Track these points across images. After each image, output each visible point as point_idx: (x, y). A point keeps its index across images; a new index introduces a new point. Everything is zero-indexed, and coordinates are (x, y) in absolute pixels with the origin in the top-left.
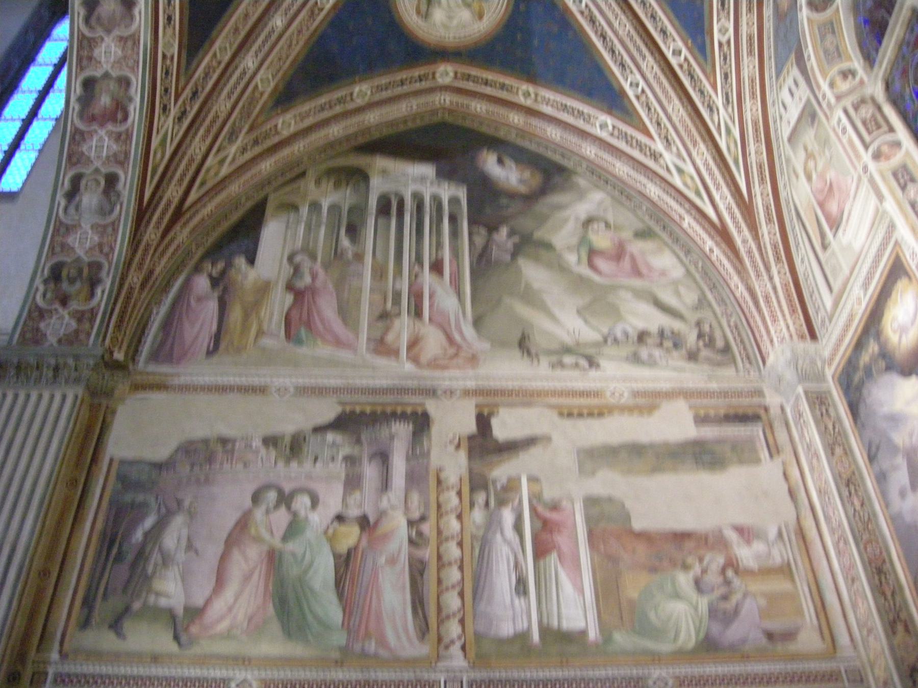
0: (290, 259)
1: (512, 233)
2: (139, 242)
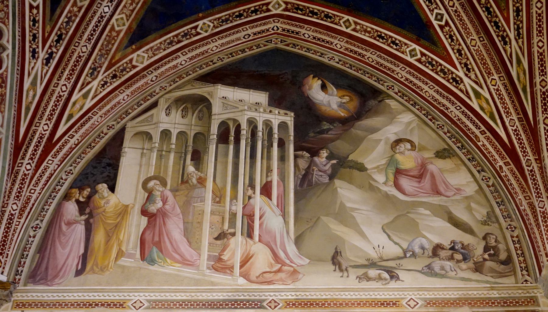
1: (329, 158)
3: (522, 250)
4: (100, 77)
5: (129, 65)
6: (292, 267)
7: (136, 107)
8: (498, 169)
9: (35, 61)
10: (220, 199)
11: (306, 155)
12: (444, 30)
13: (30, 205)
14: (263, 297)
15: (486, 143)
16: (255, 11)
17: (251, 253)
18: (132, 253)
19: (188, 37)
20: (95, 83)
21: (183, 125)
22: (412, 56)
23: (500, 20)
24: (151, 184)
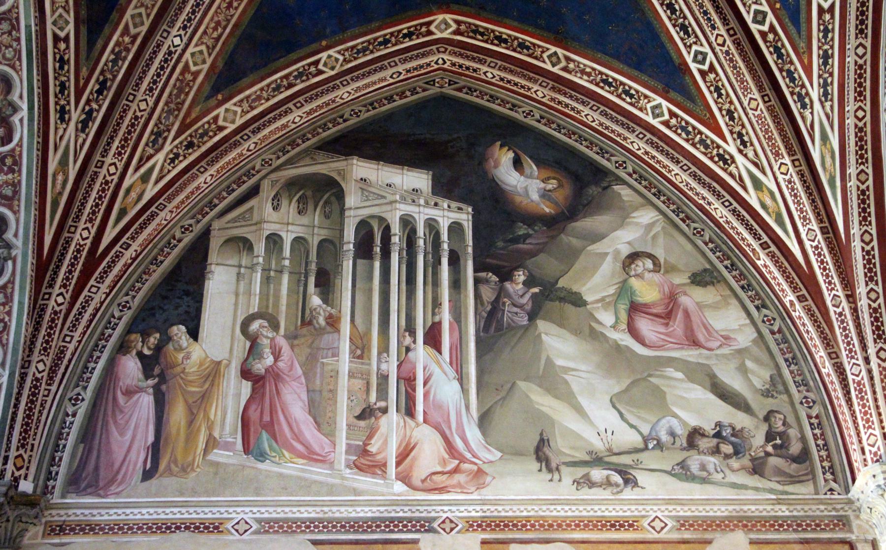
0: (245, 326)
1: (528, 284)
2: (43, 309)
3: (824, 440)
4: (167, 147)
5: (213, 126)
6: (476, 464)
7: (225, 194)
8: (788, 305)
9: (65, 126)
10: (363, 352)
12: (708, 79)
13: (65, 362)
14: (433, 514)
15: (769, 263)
16: (409, 35)
18: (229, 442)
19: (304, 78)
20: (160, 157)
22: (655, 116)
23: (796, 69)
24: (255, 326)
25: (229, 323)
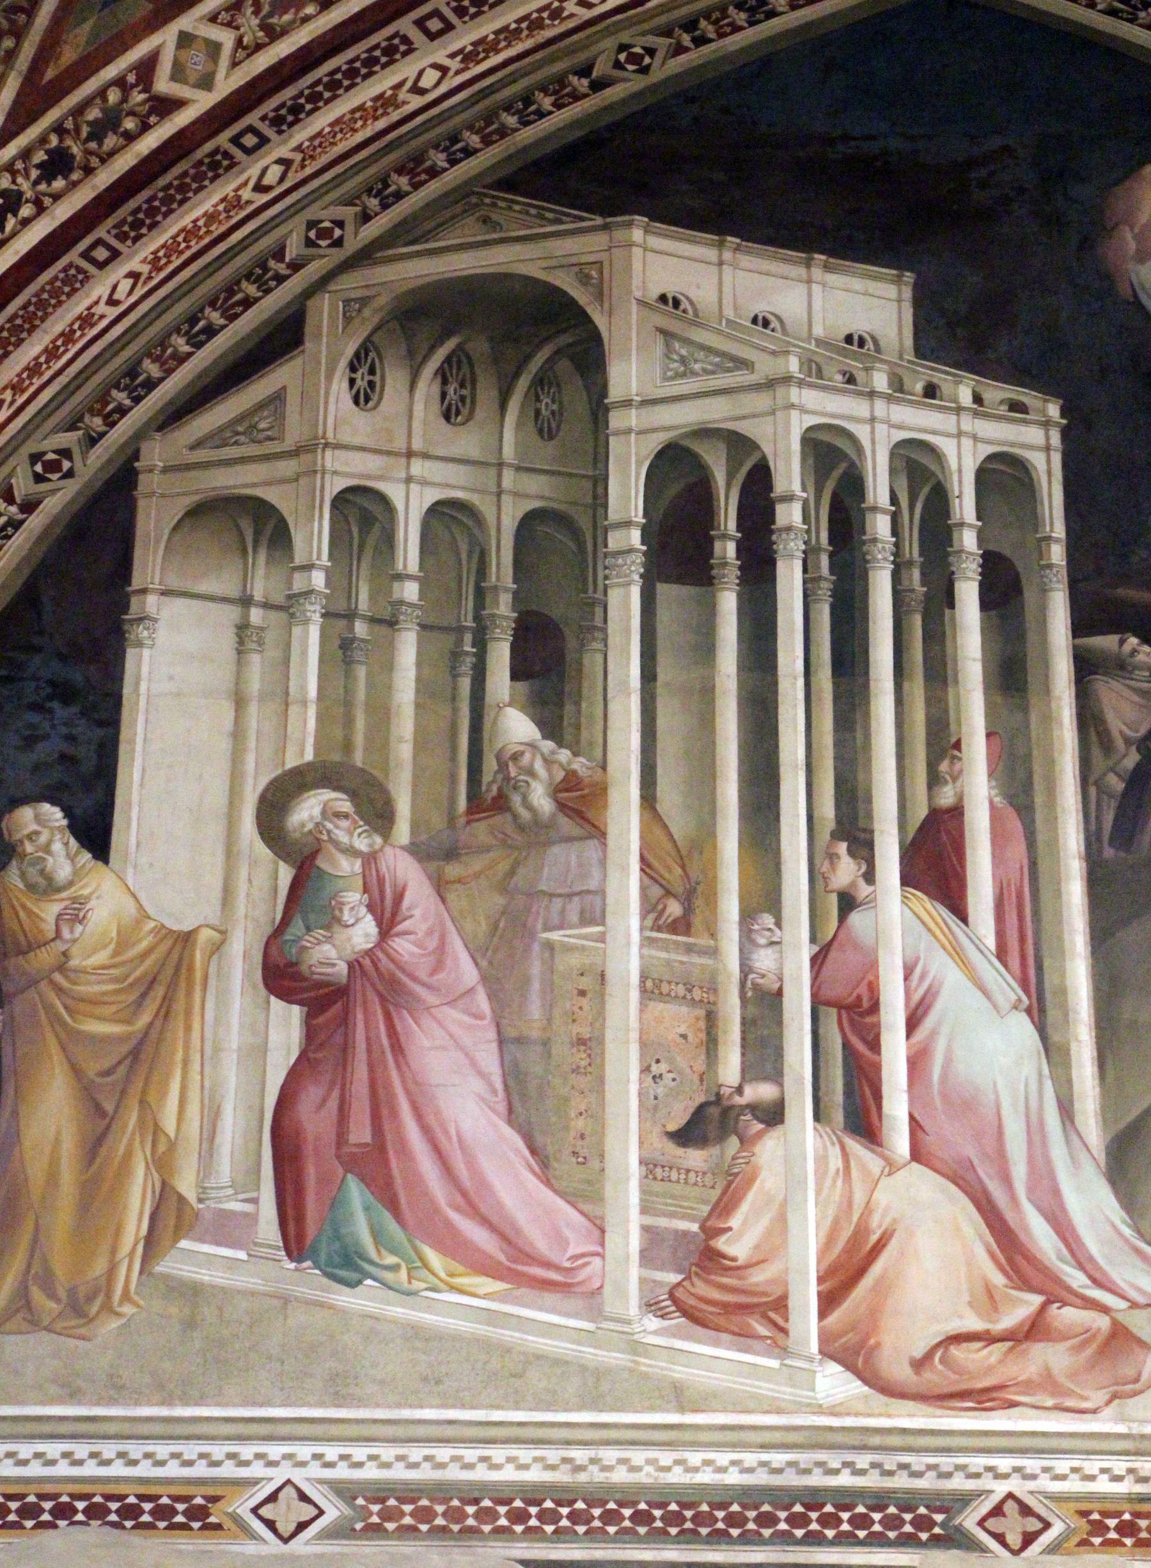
5: (138, 97)
6: (1105, 1309)
7: (180, 343)
10: (688, 910)
11: (1141, 657)
14: (959, 1483)
17: (877, 1225)
18: (233, 1213)
21: (462, 468)
25: (218, 797)
